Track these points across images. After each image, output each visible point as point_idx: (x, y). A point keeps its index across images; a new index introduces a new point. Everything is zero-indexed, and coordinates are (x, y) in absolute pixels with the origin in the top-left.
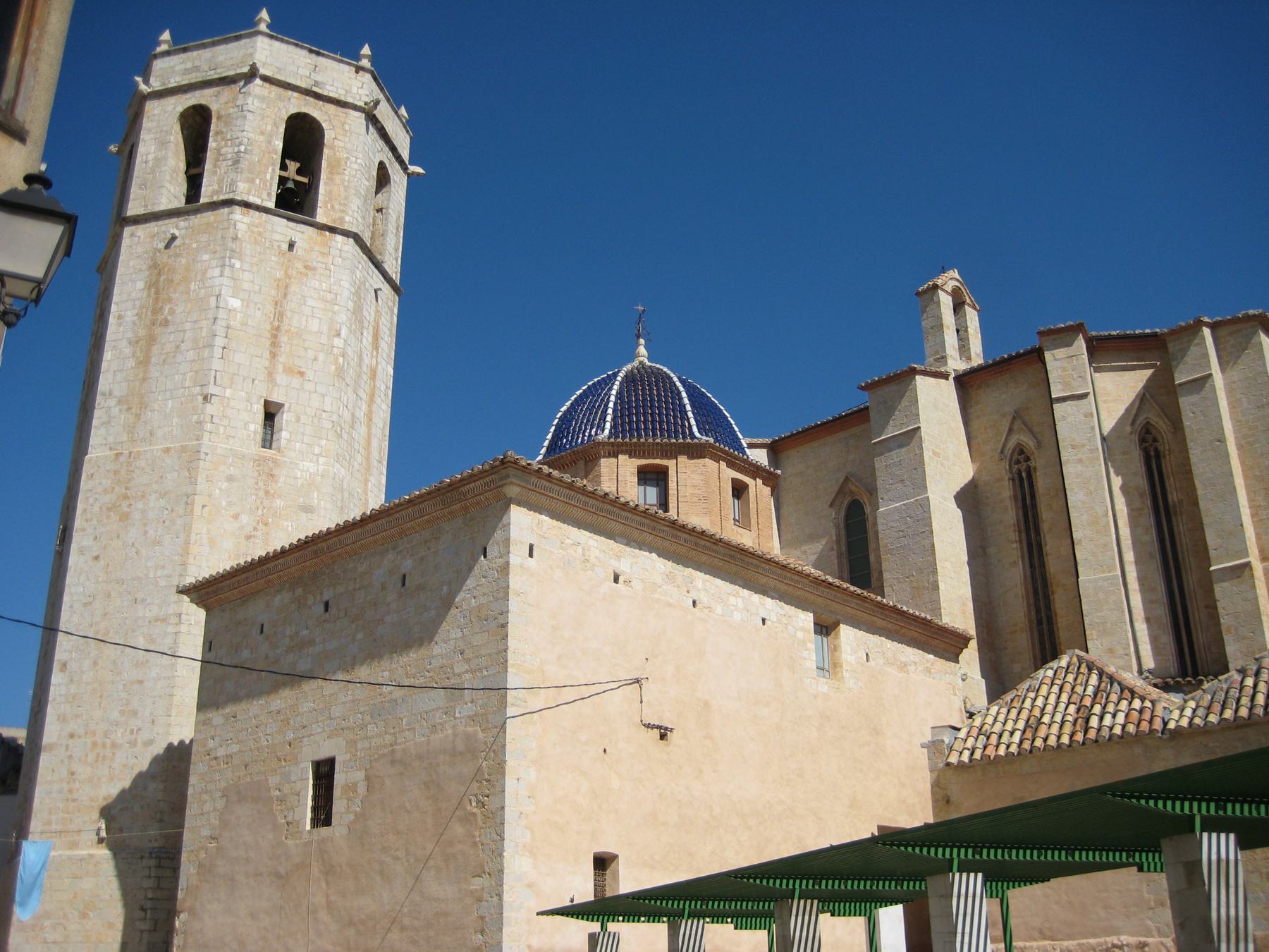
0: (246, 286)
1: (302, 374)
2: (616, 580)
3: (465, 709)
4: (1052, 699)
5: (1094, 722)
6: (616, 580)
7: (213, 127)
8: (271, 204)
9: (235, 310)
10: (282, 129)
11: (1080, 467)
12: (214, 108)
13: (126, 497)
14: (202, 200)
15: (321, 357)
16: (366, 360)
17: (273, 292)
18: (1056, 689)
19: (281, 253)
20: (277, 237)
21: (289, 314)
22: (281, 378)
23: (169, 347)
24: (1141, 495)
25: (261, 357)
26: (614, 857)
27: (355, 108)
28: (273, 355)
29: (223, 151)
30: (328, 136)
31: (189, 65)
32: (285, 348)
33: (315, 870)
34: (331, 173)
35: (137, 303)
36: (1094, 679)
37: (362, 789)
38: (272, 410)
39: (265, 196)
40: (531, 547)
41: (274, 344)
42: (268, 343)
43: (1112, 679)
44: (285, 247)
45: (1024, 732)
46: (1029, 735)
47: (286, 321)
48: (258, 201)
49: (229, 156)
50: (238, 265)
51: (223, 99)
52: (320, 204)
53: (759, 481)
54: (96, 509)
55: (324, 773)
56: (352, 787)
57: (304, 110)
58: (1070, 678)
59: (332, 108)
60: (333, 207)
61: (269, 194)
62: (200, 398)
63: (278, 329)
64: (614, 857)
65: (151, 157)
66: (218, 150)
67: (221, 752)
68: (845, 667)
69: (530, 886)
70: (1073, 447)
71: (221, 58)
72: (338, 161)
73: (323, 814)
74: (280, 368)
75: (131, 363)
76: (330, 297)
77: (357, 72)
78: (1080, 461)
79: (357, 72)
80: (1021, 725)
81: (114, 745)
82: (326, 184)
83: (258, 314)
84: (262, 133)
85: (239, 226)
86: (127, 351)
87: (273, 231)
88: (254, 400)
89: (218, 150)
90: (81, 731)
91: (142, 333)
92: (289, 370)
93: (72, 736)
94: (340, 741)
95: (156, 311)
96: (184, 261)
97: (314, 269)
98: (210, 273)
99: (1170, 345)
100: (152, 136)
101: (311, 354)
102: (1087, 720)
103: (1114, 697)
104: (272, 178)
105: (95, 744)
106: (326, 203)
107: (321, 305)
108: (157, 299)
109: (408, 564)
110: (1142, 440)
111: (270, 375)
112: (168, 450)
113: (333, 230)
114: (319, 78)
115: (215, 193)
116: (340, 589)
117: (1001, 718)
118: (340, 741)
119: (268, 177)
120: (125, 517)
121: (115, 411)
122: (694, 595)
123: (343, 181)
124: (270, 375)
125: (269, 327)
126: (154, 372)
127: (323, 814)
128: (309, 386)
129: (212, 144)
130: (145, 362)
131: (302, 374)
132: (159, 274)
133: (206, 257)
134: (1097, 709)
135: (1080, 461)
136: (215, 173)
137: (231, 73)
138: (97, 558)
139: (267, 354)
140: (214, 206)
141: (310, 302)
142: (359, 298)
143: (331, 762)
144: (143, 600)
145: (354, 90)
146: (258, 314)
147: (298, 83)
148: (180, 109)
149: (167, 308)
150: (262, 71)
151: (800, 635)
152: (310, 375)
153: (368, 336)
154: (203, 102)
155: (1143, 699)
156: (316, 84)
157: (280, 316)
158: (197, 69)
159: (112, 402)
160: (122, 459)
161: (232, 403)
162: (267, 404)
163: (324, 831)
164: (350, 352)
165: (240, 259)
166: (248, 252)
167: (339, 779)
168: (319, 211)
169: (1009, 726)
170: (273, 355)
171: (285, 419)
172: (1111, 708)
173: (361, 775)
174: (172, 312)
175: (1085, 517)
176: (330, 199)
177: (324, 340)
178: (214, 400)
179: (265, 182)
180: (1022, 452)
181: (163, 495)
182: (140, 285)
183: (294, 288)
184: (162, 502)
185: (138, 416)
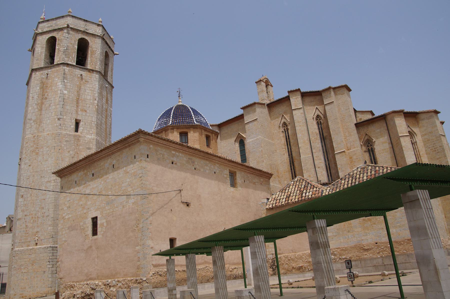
1: (86, 111)
2: (172, 163)
3: (132, 201)
4: (293, 189)
5: (304, 195)
6: (172, 163)
7: (57, 42)
8: (75, 64)
10: (77, 43)
11: (300, 128)
12: (57, 37)
13: (37, 148)
14: (55, 63)
15: (91, 106)
16: (104, 107)
17: (76, 89)
18: (294, 187)
19: (78, 78)
20: (77, 73)
22: (80, 113)
23: (47, 105)
24: (317, 134)
26: (176, 239)
28: (77, 106)
29: (60, 49)
30: (91, 44)
33: (94, 248)
36: (304, 183)
37: (105, 224)
40: (148, 155)
43: (308, 183)
44: (79, 76)
45: (286, 198)
46: (287, 199)
47: (81, 97)
48: (71, 63)
50: (66, 81)
51: (59, 34)
53: (213, 135)
54: (29, 152)
55: (95, 220)
56: (102, 224)
58: (298, 183)
62: (57, 119)
63: (78, 99)
64: (176, 239)
65: (39, 51)
66: (59, 49)
67: (67, 217)
68: (238, 184)
69: (152, 248)
70: (298, 122)
71: (58, 23)
72: (94, 51)
73: (95, 233)
74: (79, 110)
75: (37, 110)
76: (93, 89)
78: (300, 126)
80: (285, 197)
81: (38, 217)
83: (72, 95)
84: (71, 44)
85: (66, 70)
86: (35, 107)
89: (59, 49)
90: (28, 214)
91: (39, 102)
92: (82, 110)
93: (26, 216)
94: (99, 212)
95: (43, 95)
96: (50, 81)
97: (88, 82)
98: (58, 84)
99: (323, 94)
101: (88, 106)
102: (302, 194)
103: (309, 188)
105: (32, 217)
106: (90, 63)
107: (90, 92)
108: (43, 92)
109: (114, 162)
110: (317, 120)
111: (77, 112)
112: (48, 134)
113: (93, 70)
115: (58, 61)
116: (96, 170)
117: (280, 195)
118: (99, 212)
120: (37, 154)
121: (33, 124)
122: (195, 166)
124: (77, 112)
126: (43, 112)
127: (95, 233)
128: (88, 115)
129: (57, 47)
130: (41, 110)
131: (86, 111)
132: (43, 85)
133: (57, 79)
134: (305, 191)
135: (300, 126)
136: (58, 56)
137: (62, 27)
138: (30, 166)
140: (58, 65)
141: (87, 91)
143: (96, 218)
144: (44, 177)
145: (97, 31)
146: (72, 95)
147: (81, 29)
148: (47, 38)
149: (46, 94)
150: (70, 26)
151: (225, 176)
152: (88, 111)
153: (104, 100)
154: (54, 35)
155: (316, 188)
156: (86, 29)
157: (79, 95)
159: (32, 122)
160: (35, 137)
162: (76, 120)
163: (95, 237)
164: (99, 104)
167: (99, 222)
169: (282, 197)
170: (77, 106)
171: (81, 124)
172: (308, 191)
173: (104, 221)
174: (48, 95)
175: (302, 141)
178: (61, 119)
179: (72, 57)
180: (285, 124)
181: (48, 147)
182: (38, 88)
183: (82, 87)
184: (48, 149)
185: (39, 125)
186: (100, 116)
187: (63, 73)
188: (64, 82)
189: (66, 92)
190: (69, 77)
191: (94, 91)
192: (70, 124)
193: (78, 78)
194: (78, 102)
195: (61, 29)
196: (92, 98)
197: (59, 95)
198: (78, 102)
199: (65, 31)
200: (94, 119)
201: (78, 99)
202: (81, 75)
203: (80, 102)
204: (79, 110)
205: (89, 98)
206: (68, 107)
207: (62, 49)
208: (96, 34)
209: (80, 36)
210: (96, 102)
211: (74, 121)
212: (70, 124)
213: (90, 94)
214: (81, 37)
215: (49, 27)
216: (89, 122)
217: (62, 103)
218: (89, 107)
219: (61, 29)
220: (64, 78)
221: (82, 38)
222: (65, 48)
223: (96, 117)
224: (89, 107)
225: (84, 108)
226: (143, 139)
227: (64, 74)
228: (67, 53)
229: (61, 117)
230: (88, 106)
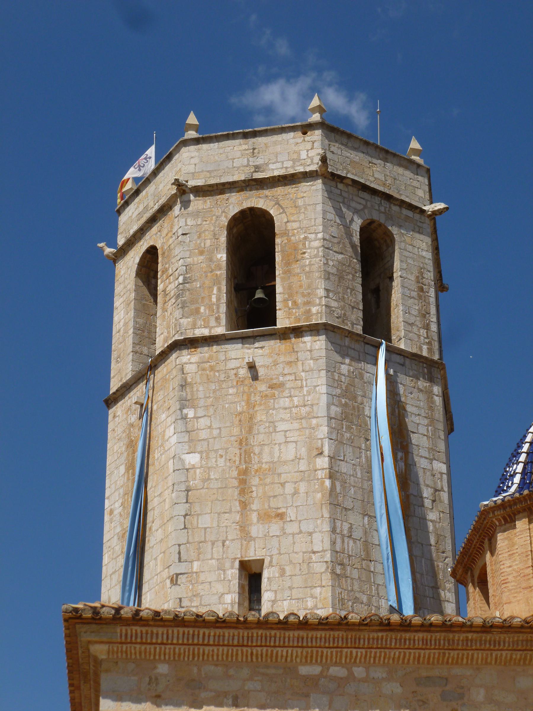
0: (203, 435)
1: (281, 516)
9: (194, 467)
10: (223, 239)
15: (303, 487)
17: (236, 431)
19: (240, 382)
20: (232, 364)
21: (257, 450)
22: (256, 530)
25: (230, 512)
27: (308, 176)
30: (279, 222)
31: (141, 208)
32: (257, 491)
34: (288, 264)
35: (121, 491)
38: (255, 570)
39: (213, 323)
41: (242, 492)
42: (236, 493)
44: (244, 372)
48: (206, 332)
49: (172, 294)
50: (191, 413)
52: (279, 306)
57: (246, 205)
59: (280, 191)
60: (295, 303)
61: (218, 319)
62: (168, 582)
63: (245, 472)
77: (305, 133)
79: (305, 133)
82: (283, 279)
83: (221, 462)
84: (201, 253)
87: (226, 360)
88: (228, 565)
89: (164, 291)
92: (266, 517)
97: (282, 385)
100: (121, 300)
101: (289, 488)
104: (218, 299)
107: (296, 425)
114: (259, 161)
119: (214, 299)
123: (303, 267)
124: (244, 529)
125: (235, 473)
128: (292, 528)
129: (160, 287)
131: (281, 516)
136: (164, 316)
139: (237, 507)
140: (165, 355)
141: (282, 426)
142: (354, 398)
145: (304, 155)
146: (221, 462)
147: (236, 178)
148: (137, 260)
150: (191, 183)
152: (291, 513)
156: (257, 169)
158: (146, 208)
161: (202, 577)
164: (344, 468)
165: (194, 407)
166: (201, 395)
168: (279, 314)
170: (244, 505)
176: (291, 295)
177: (303, 466)
178: (182, 579)
179: (210, 307)
182: (122, 469)
183: (260, 416)
186: (355, 518)
187: (176, 383)
188: (184, 418)
189: (193, 459)
190: (201, 391)
191: (309, 416)
192: (219, 588)
193: (240, 382)
194: (244, 486)
195: (164, 210)
196: (303, 451)
197: (170, 484)
198: (244, 486)
199: (177, 209)
200: (321, 541)
201: (245, 472)
202: (252, 367)
203: (255, 481)
204: (254, 517)
205: (291, 456)
206: (205, 521)
207: (172, 288)
208: (301, 169)
209: (235, 203)
210: (323, 462)
211: (233, 573)
212: (219, 588)
213: (293, 436)
214: (236, 210)
215: (140, 215)
216: (298, 558)
217: (182, 509)
218: (296, 492)
219: (164, 210)
220: (184, 403)
221: (243, 213)
222: (181, 279)
223: (326, 527)
224: (296, 492)
225: (274, 503)
226: (105, 647)
227: (183, 387)
228: (187, 296)
229: (181, 568)
230: (289, 488)
